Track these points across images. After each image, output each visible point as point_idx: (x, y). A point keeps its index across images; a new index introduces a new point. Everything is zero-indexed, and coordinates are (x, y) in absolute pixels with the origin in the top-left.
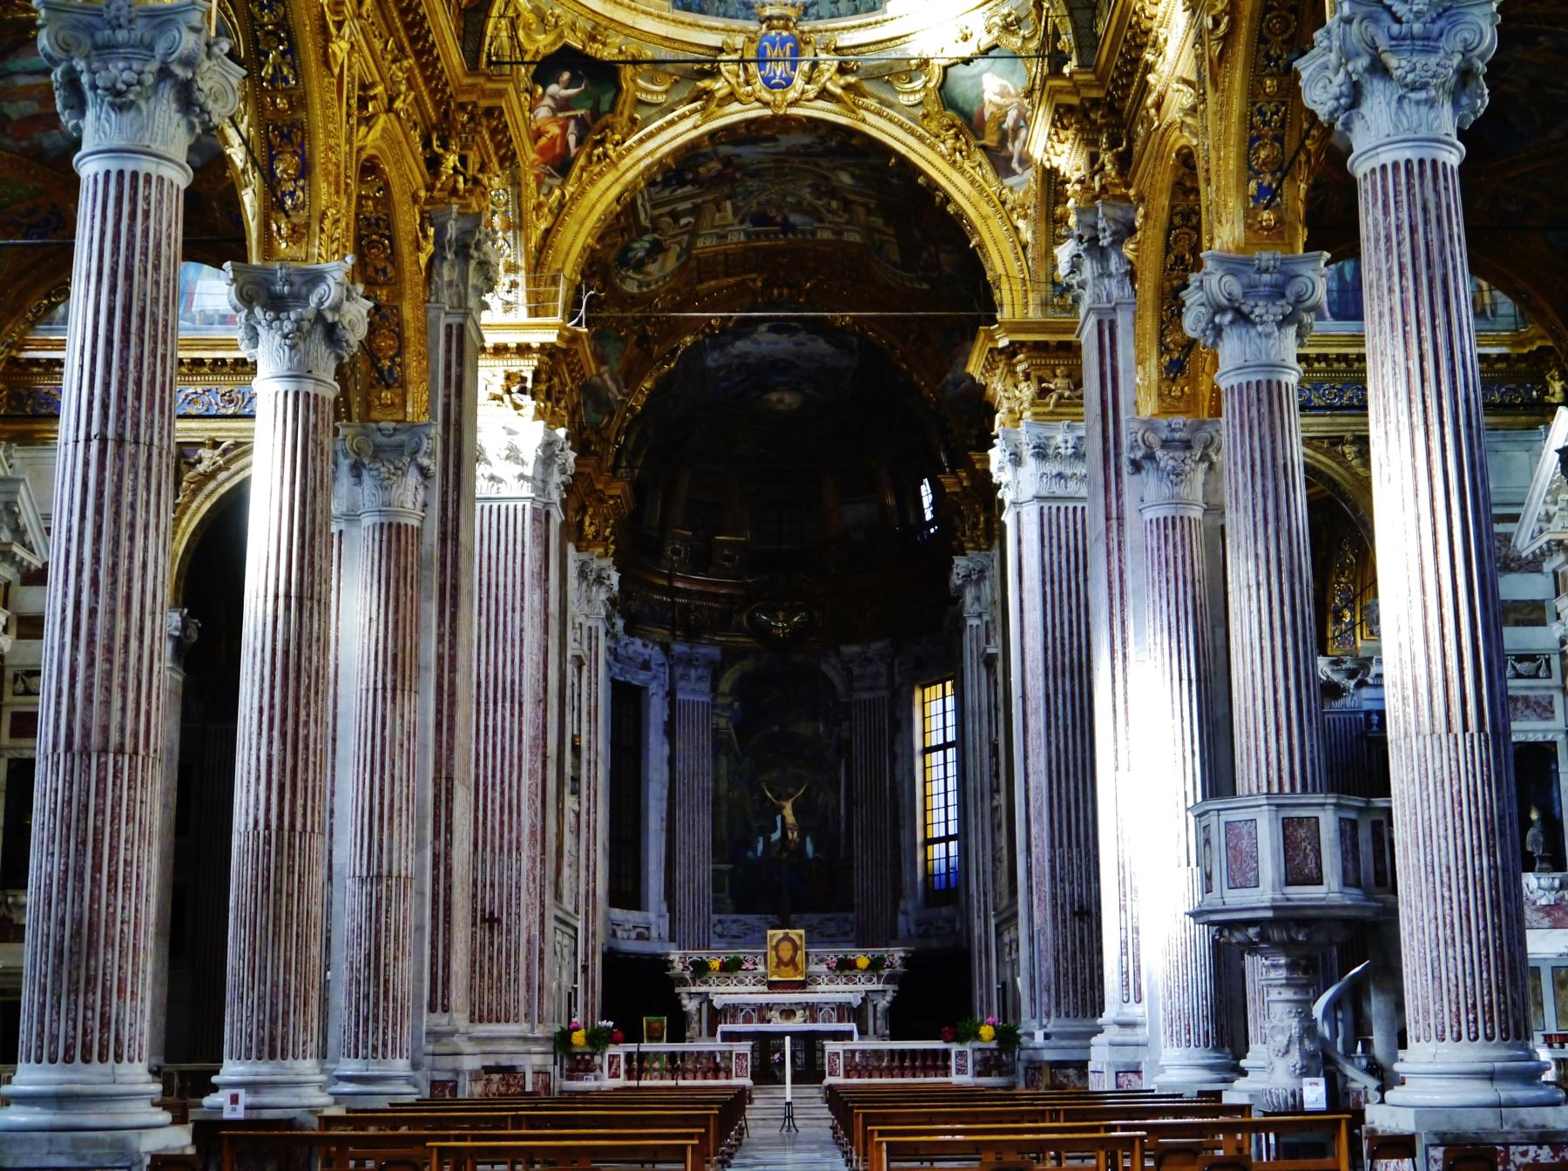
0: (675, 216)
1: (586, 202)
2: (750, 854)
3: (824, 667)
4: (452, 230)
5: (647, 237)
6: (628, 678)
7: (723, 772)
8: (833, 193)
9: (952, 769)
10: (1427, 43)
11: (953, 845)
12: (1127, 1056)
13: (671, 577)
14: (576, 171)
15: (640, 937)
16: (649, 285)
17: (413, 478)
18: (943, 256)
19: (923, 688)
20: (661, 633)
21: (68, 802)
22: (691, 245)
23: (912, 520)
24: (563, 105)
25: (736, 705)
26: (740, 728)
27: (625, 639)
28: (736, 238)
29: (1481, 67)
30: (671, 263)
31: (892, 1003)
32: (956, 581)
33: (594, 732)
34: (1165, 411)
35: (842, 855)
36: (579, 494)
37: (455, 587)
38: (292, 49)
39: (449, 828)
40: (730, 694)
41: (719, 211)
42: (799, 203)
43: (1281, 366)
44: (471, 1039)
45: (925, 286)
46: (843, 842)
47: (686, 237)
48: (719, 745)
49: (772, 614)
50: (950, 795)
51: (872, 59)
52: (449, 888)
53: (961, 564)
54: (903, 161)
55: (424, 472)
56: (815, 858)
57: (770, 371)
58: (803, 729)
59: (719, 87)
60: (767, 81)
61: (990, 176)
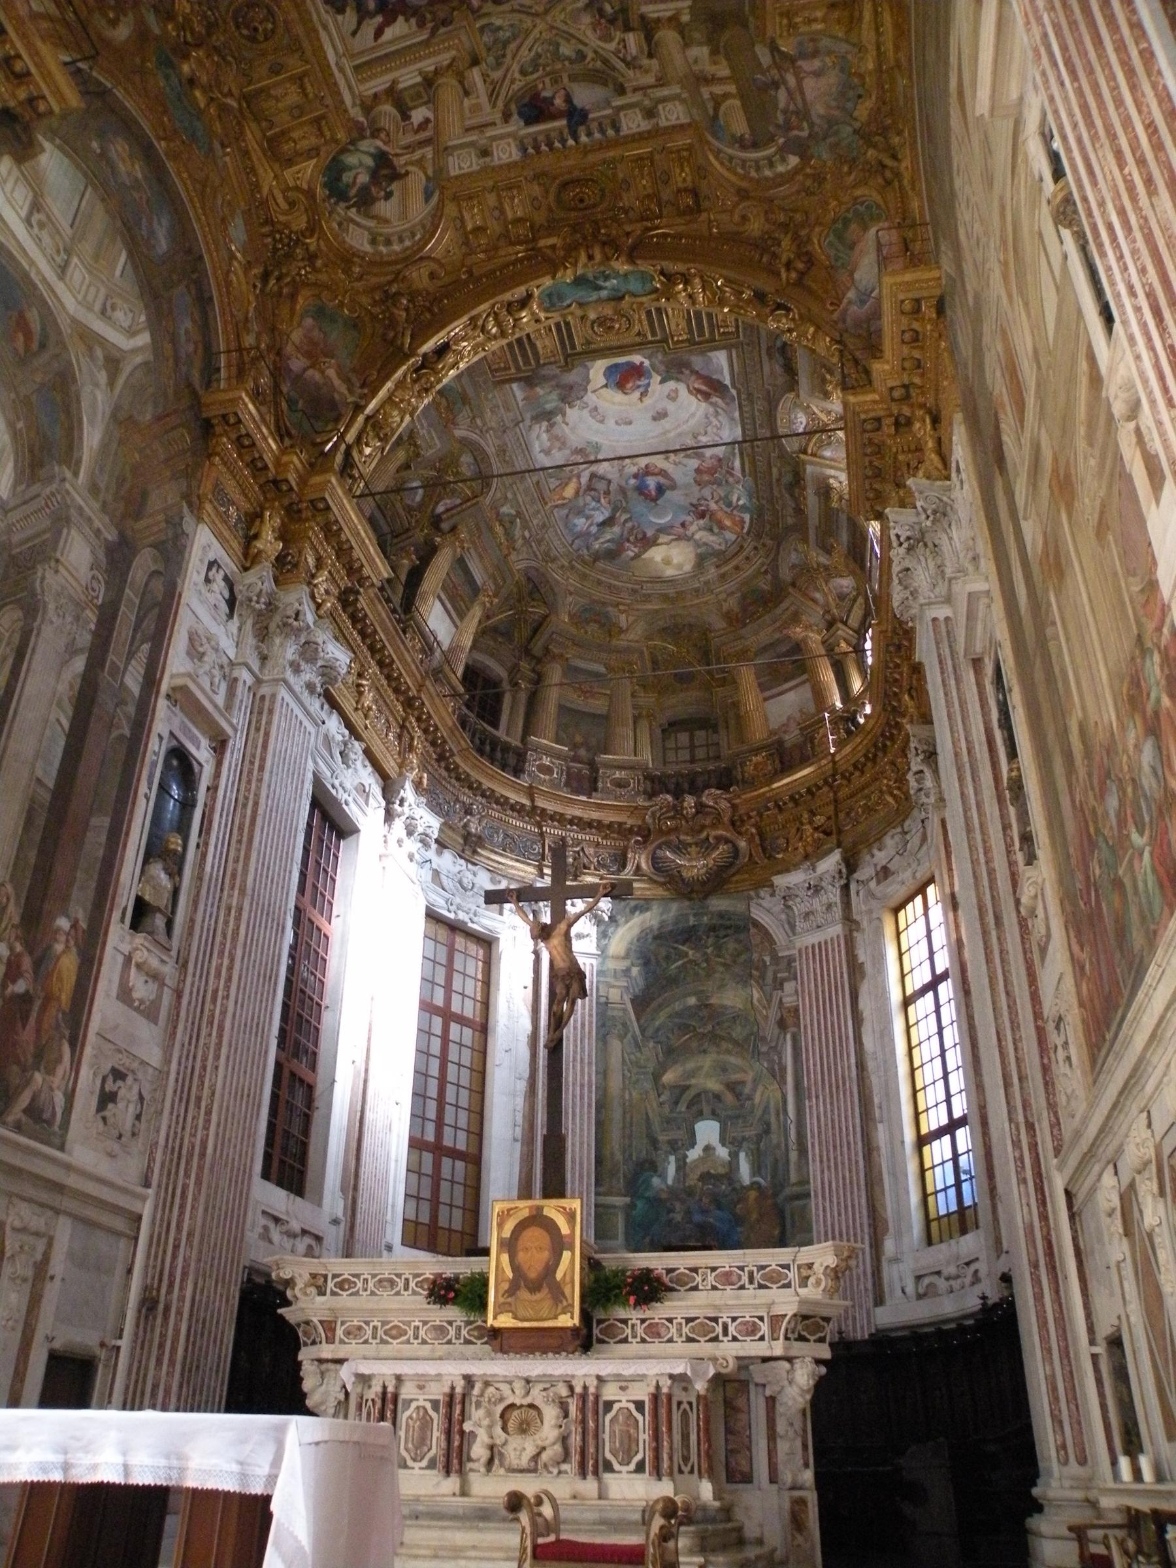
2: (656, 1181)
5: (367, 145)
6: (462, 916)
7: (615, 1060)
9: (949, 1013)
11: (962, 1135)
16: (388, 242)
18: (809, 84)
19: (896, 911)
22: (440, 170)
25: (635, 971)
31: (821, 1389)
35: (793, 1177)
40: (626, 956)
41: (467, 93)
42: (581, 56)
45: (794, 160)
46: (793, 1156)
47: (428, 151)
50: (950, 1055)
56: (755, 1185)
58: (731, 998)
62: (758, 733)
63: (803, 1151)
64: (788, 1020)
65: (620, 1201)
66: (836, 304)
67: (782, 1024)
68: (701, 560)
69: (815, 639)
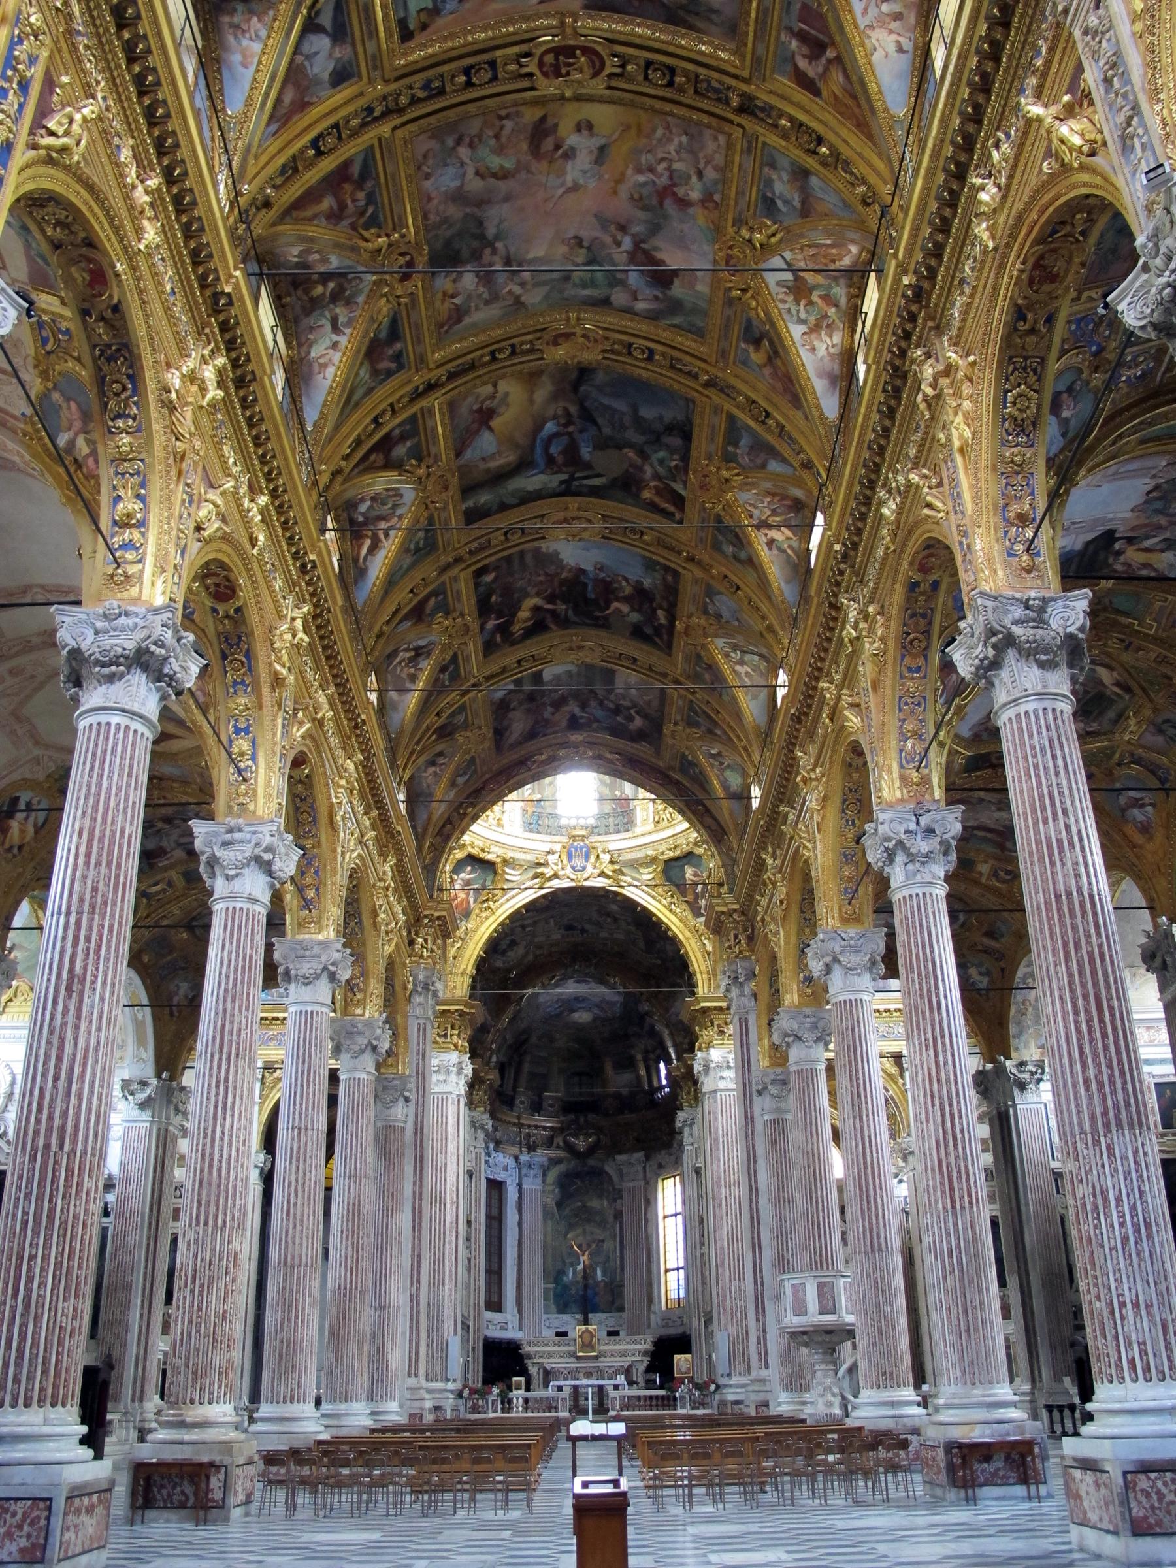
0: (523, 927)
1: (479, 933)
3: (607, 1168)
4: (421, 977)
7: (549, 1229)
8: (608, 915)
10: (856, 949)
11: (682, 1272)
12: (761, 1397)
13: (519, 1118)
14: (473, 916)
15: (502, 1328)
17: (401, 1101)
20: (515, 1150)
21: (284, 1288)
23: (656, 1084)
24: (468, 883)
26: (559, 1204)
27: (494, 1154)
28: (556, 936)
29: (879, 959)
30: (520, 951)
32: (678, 1124)
33: (478, 1211)
34: (772, 1065)
36: (473, 1084)
37: (422, 1157)
38: (360, 921)
39: (418, 1281)
43: (817, 1061)
44: (429, 1391)
48: (547, 1214)
49: (576, 1136)
51: (629, 856)
52: (418, 1313)
53: (681, 1116)
54: (645, 909)
55: (407, 1100)
57: (577, 1002)
58: (595, 1203)
59: (548, 872)
60: (573, 868)
61: (690, 917)
62: (611, 1090)
63: (622, 1269)
64: (618, 1215)
65: (552, 1286)
66: (667, 1010)
67: (616, 1217)
68: (595, 1019)
69: (639, 1057)
